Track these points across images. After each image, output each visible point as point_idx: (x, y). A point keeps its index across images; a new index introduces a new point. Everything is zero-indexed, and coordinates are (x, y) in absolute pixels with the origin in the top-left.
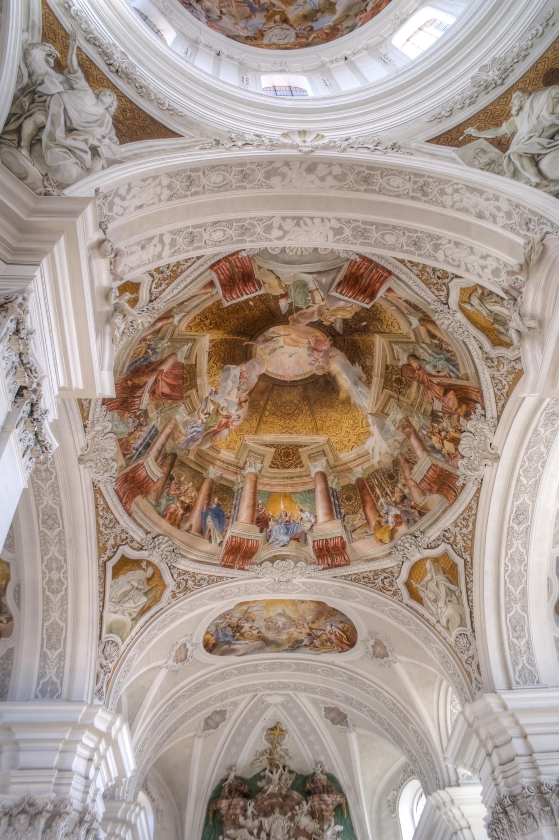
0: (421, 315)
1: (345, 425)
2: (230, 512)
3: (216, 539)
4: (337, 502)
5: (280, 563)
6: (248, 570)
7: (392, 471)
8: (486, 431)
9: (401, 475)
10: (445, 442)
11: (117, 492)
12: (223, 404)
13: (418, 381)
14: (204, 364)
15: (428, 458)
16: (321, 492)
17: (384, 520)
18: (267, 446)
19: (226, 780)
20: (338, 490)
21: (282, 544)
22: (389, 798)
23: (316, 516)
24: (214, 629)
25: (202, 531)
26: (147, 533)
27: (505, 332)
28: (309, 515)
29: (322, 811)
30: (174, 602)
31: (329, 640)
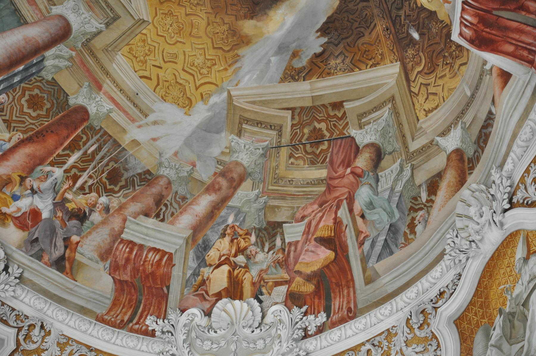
0: (470, 152)
1: (187, 48)
4: (17, 79)
7: (126, 175)
8: (276, 348)
9: (125, 196)
10: (225, 268)
13: (331, 179)
15: (181, 242)
16: (26, 40)
17: (17, 190)
20: (43, 73)
27: (493, 341)
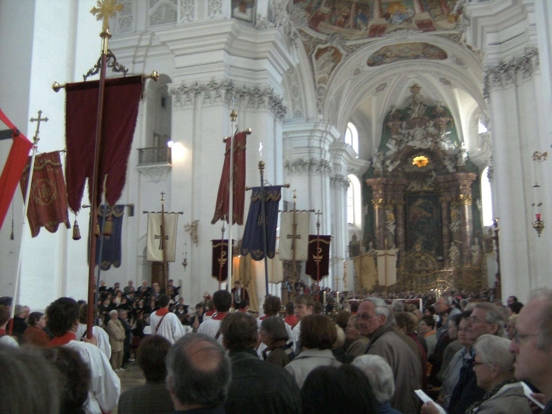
6: (383, 36)
11: (310, 27)
19: (390, 112)
21: (399, 23)
22: (476, 117)
23: (415, 11)
25: (356, 26)
26: (328, 35)
29: (440, 125)
31: (434, 55)
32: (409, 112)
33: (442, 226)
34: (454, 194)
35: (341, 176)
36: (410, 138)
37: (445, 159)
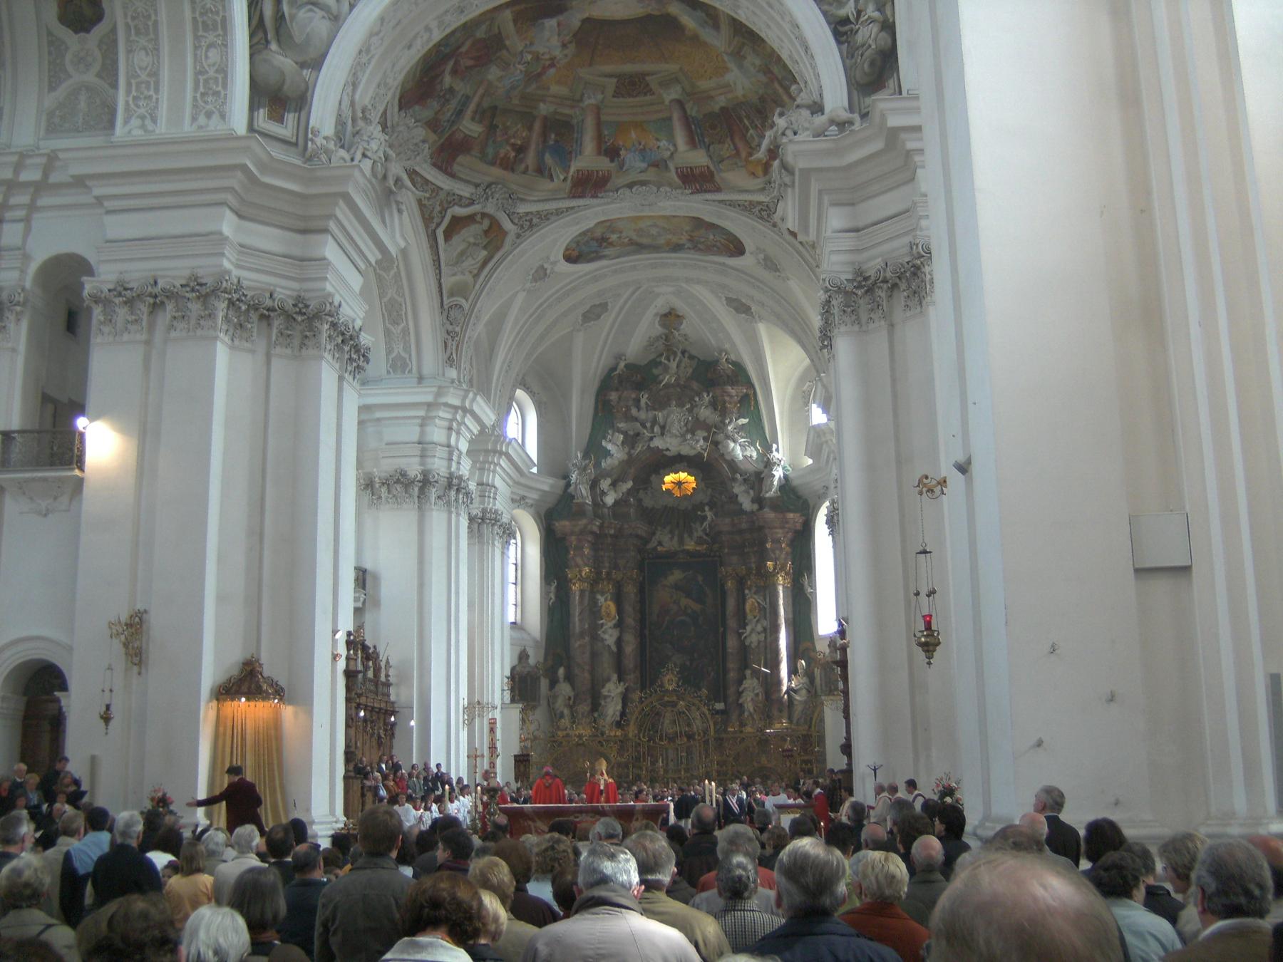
2: (572, 147)
3: (558, 177)
5: (640, 189)
6: (602, 197)
11: (435, 165)
12: (541, 50)
14: (510, 27)
18: (606, 76)
19: (614, 369)
21: (639, 170)
22: (805, 388)
23: (675, 145)
24: (574, 245)
25: (541, 170)
26: (477, 186)
28: (666, 144)
29: (725, 402)
30: (518, 241)
31: (714, 246)
32: (655, 371)
33: (724, 634)
34: (753, 560)
35: (496, 512)
36: (657, 429)
37: (734, 480)
